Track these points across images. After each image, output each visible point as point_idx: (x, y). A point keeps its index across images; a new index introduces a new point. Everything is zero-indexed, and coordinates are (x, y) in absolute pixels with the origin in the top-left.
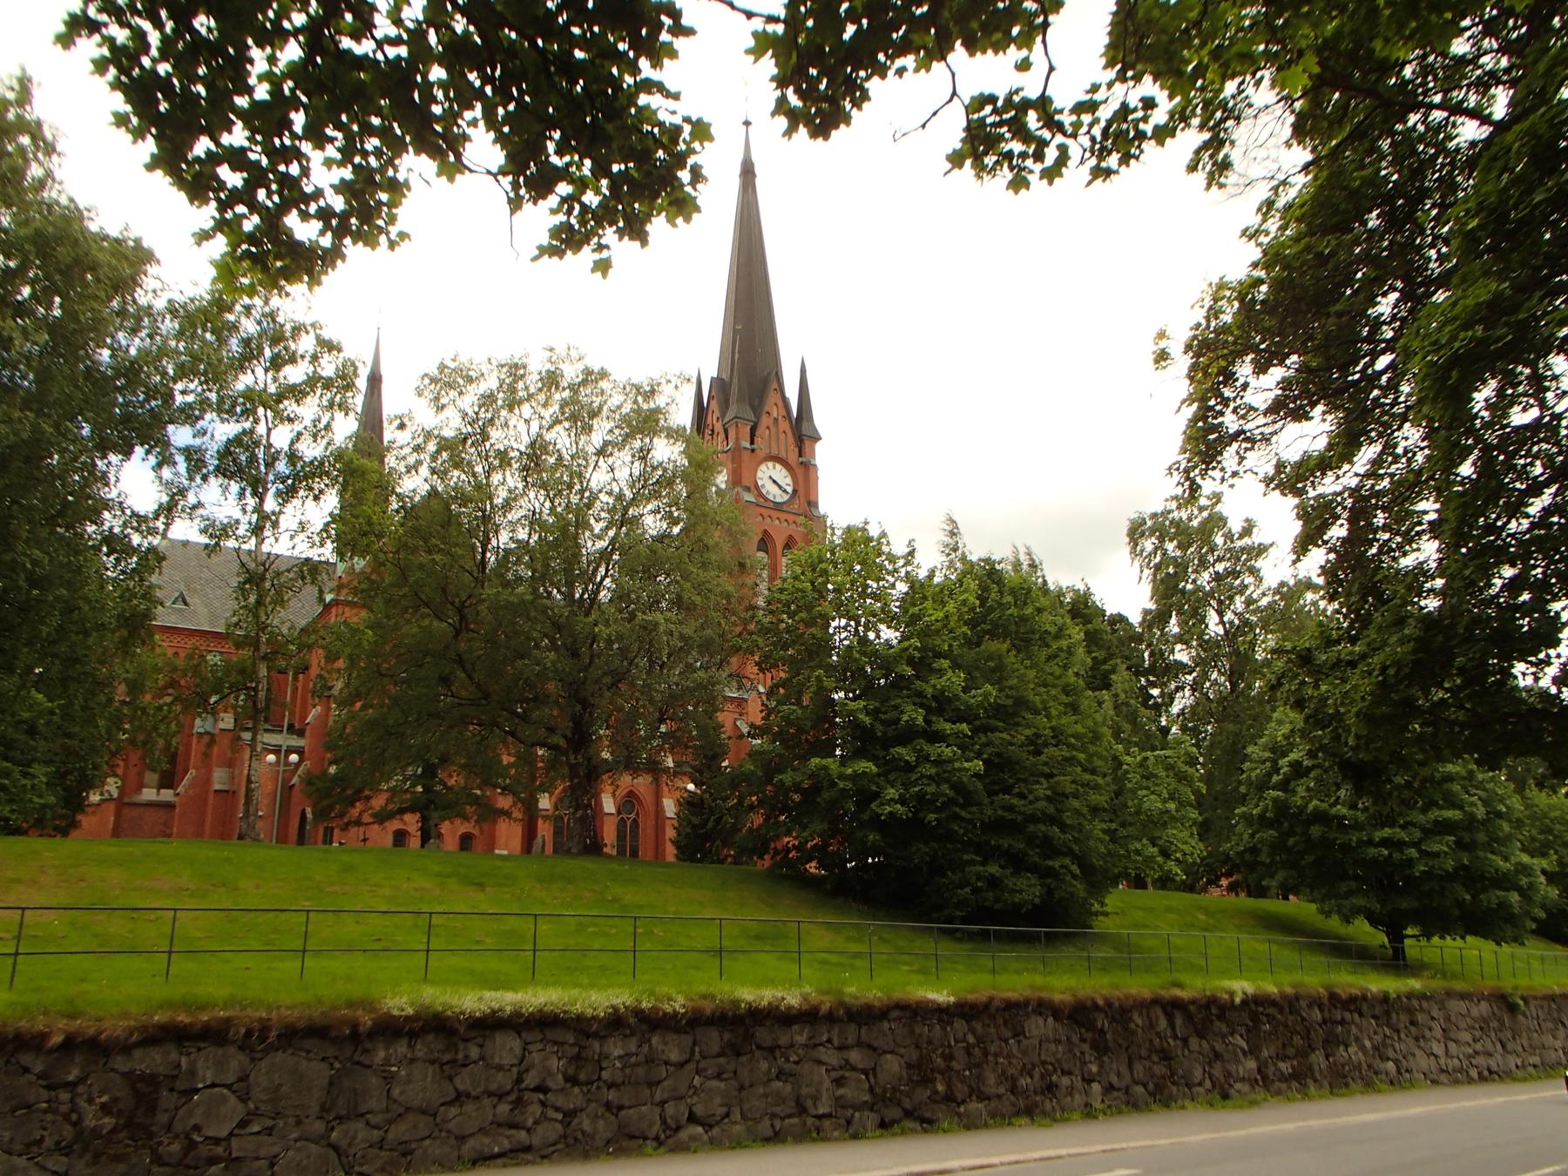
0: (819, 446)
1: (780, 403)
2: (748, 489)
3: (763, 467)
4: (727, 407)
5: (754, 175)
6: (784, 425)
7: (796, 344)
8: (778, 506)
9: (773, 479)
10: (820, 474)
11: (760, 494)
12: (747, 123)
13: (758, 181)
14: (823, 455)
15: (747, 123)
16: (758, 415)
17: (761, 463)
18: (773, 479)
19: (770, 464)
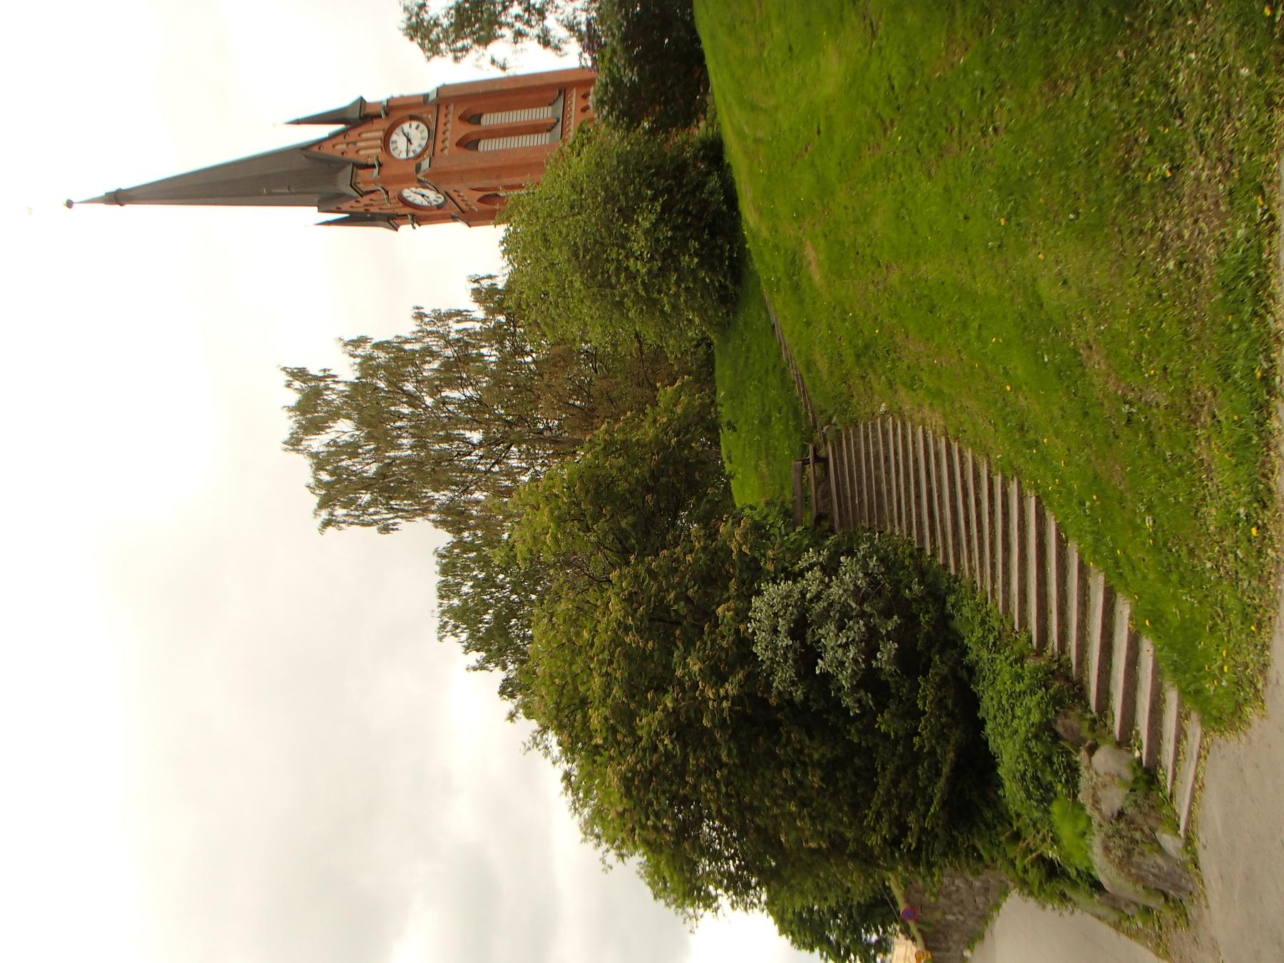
0: (369, 99)
1: (334, 141)
2: (418, 168)
3: (395, 154)
4: (344, 194)
6: (353, 135)
7: (271, 132)
8: (433, 135)
9: (410, 140)
10: (396, 94)
12: (70, 204)
13: (125, 186)
14: (377, 94)
16: (347, 163)
17: (392, 157)
18: (410, 140)
19: (392, 146)
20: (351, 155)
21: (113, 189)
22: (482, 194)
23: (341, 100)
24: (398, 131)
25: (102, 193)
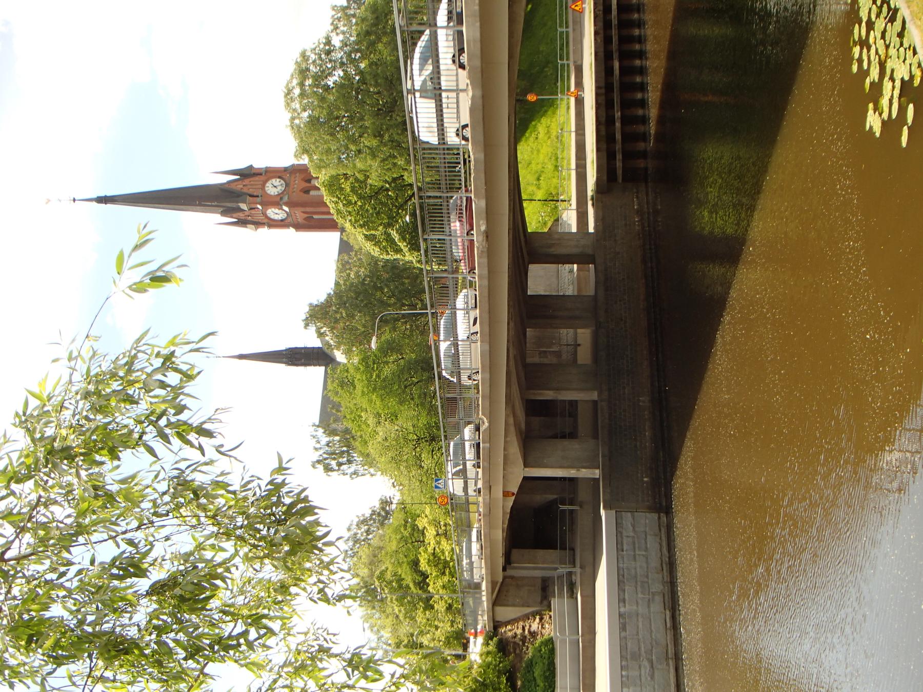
0: (256, 166)
2: (281, 199)
3: (268, 192)
5: (106, 196)
6: (247, 181)
9: (274, 187)
11: (282, 193)
13: (108, 195)
14: (260, 163)
15: (74, 200)
18: (274, 187)
20: (245, 190)
21: (103, 195)
22: (306, 215)
23: (242, 165)
24: (270, 182)
25: (95, 196)
